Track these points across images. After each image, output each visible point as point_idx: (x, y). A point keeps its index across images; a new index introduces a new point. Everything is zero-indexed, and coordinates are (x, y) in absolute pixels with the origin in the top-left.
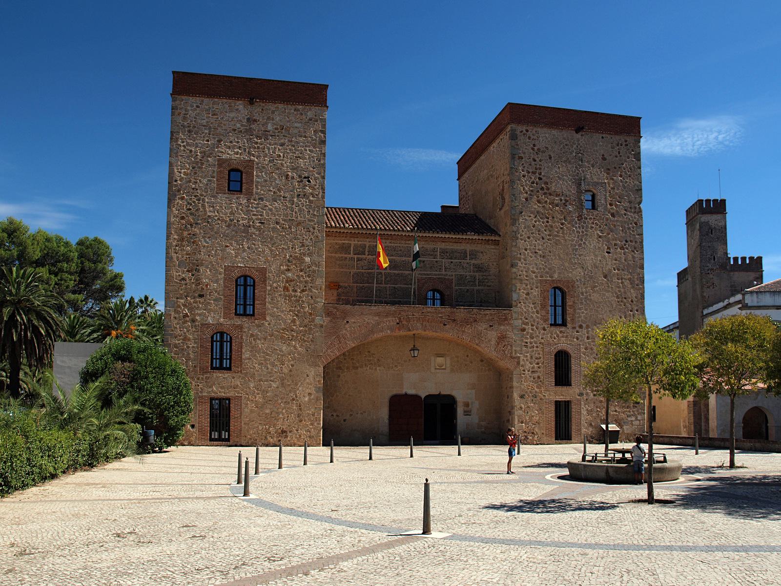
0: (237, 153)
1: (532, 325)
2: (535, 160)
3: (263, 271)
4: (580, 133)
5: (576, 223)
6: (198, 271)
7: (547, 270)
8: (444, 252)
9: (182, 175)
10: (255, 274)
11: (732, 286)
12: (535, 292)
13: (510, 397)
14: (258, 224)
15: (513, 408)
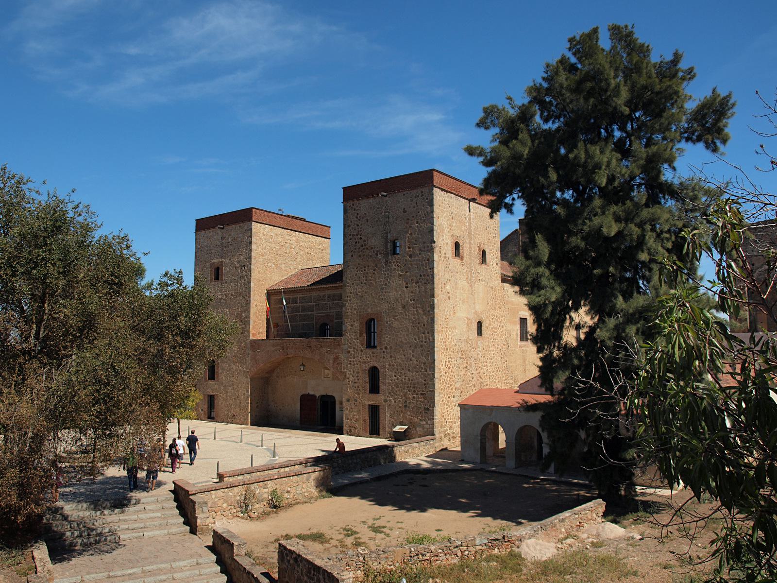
1: (354, 348)
2: (358, 225)
12: (356, 324)
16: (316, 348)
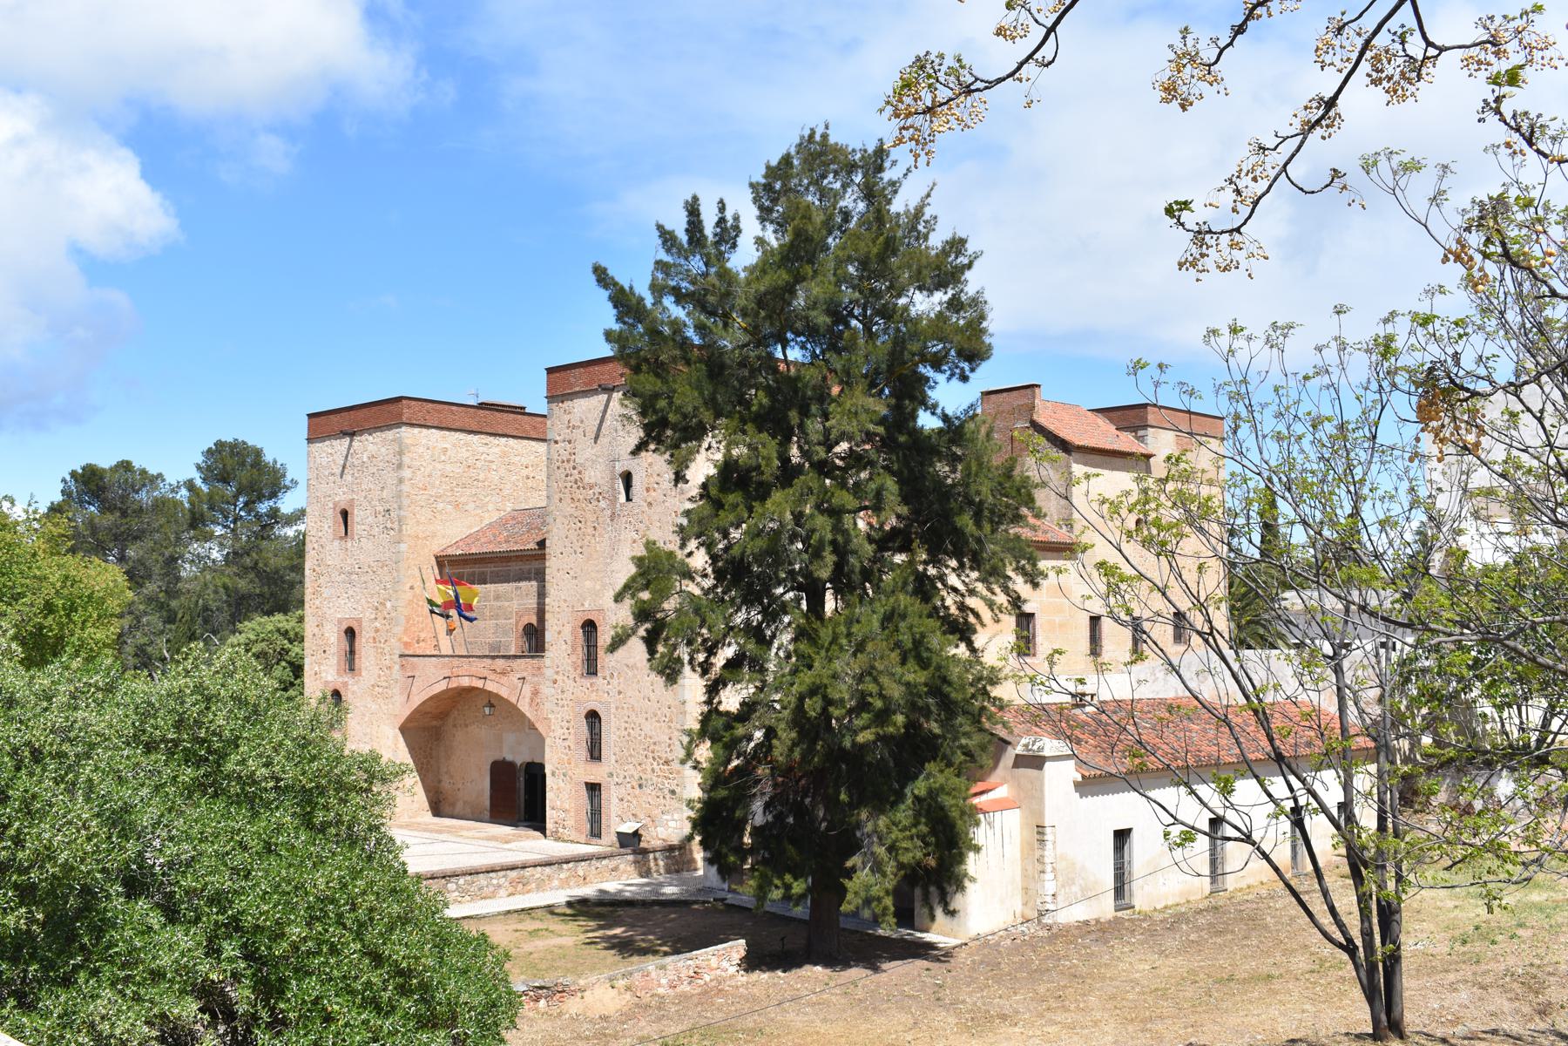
3: (359, 621)
12: (567, 630)
16: (503, 673)
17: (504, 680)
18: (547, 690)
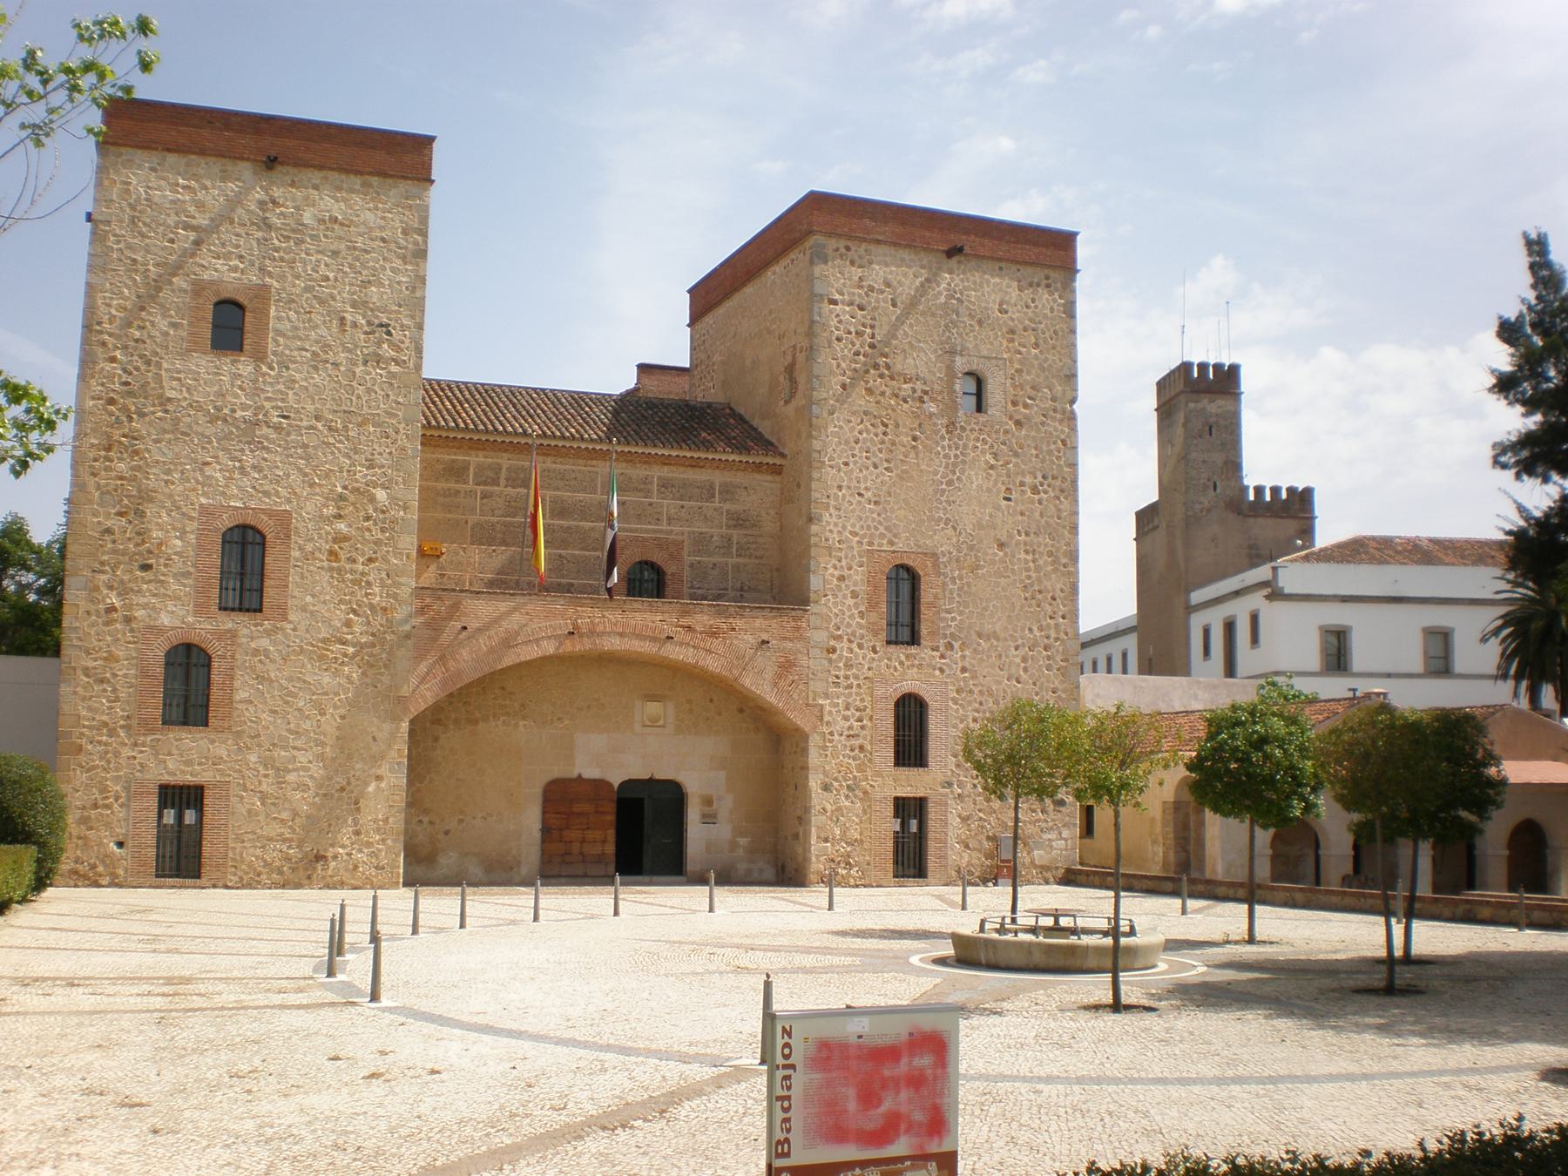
0: (235, 269)
1: (850, 641)
3: (284, 520)
4: (955, 259)
5: (943, 438)
6: (142, 515)
7: (882, 529)
8: (665, 484)
9: (114, 312)
10: (267, 525)
11: (1250, 547)
12: (858, 576)
13: (801, 787)
14: (276, 420)
15: (807, 810)
17: (715, 643)
18: (814, 662)
